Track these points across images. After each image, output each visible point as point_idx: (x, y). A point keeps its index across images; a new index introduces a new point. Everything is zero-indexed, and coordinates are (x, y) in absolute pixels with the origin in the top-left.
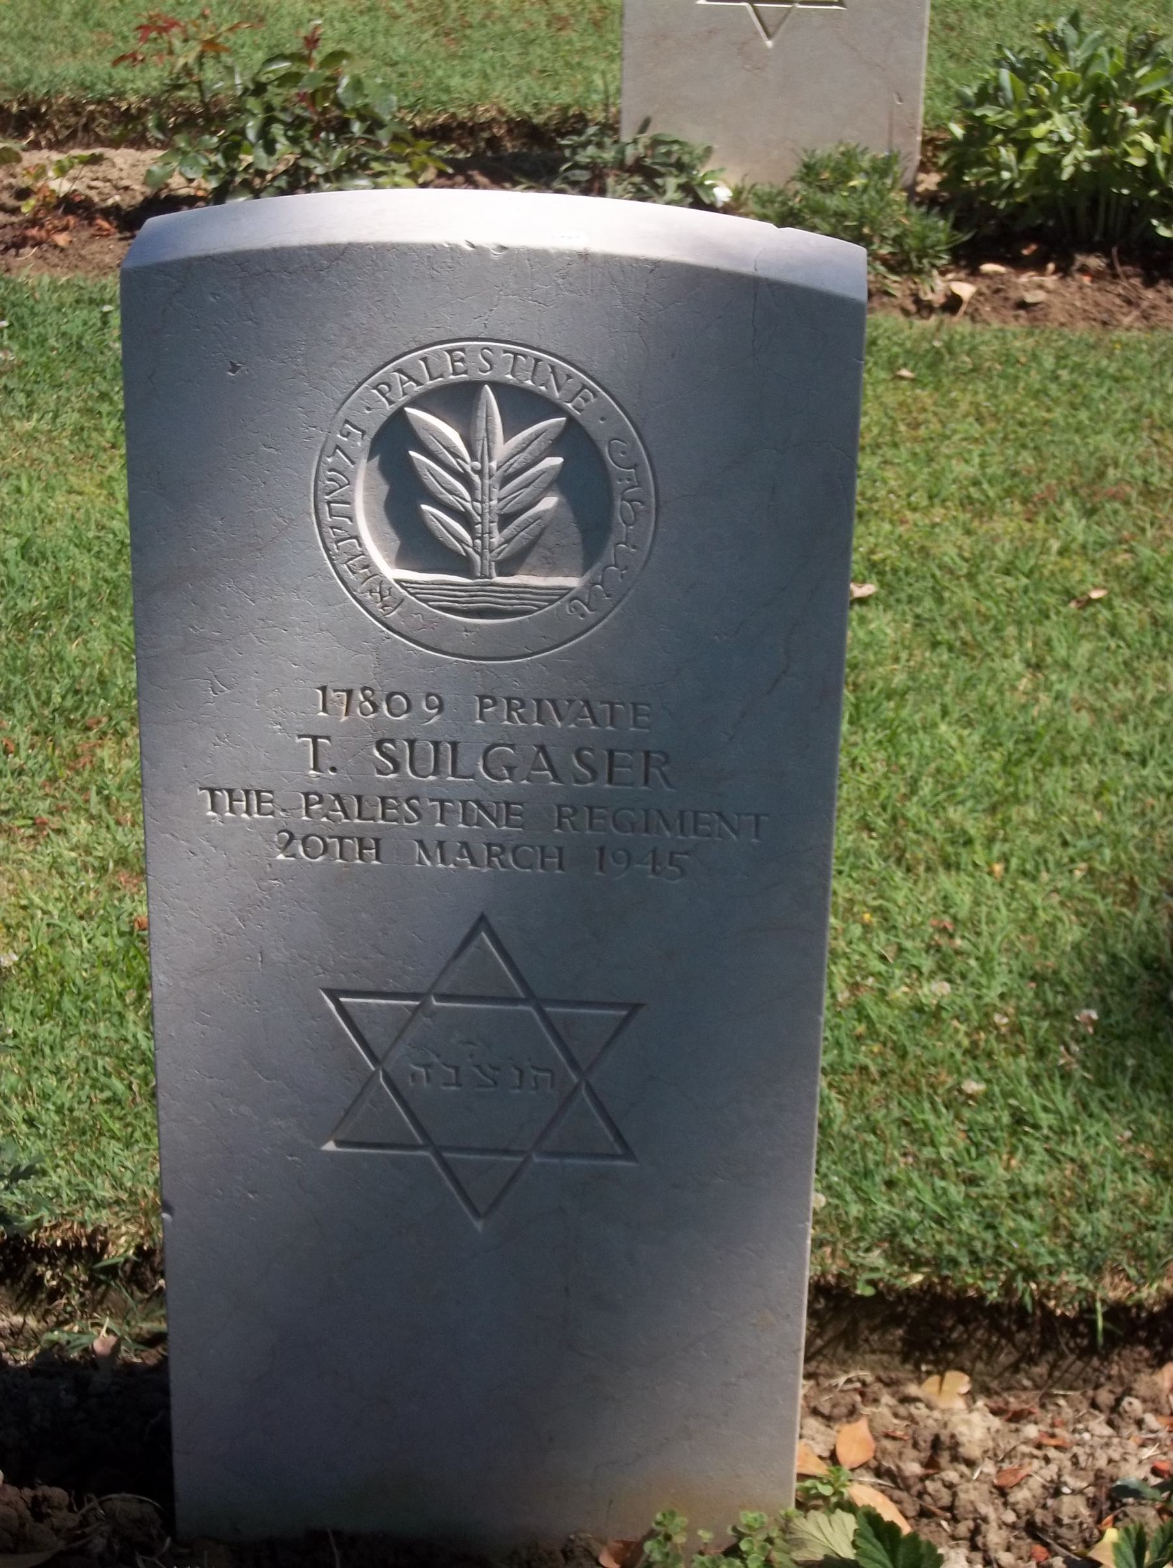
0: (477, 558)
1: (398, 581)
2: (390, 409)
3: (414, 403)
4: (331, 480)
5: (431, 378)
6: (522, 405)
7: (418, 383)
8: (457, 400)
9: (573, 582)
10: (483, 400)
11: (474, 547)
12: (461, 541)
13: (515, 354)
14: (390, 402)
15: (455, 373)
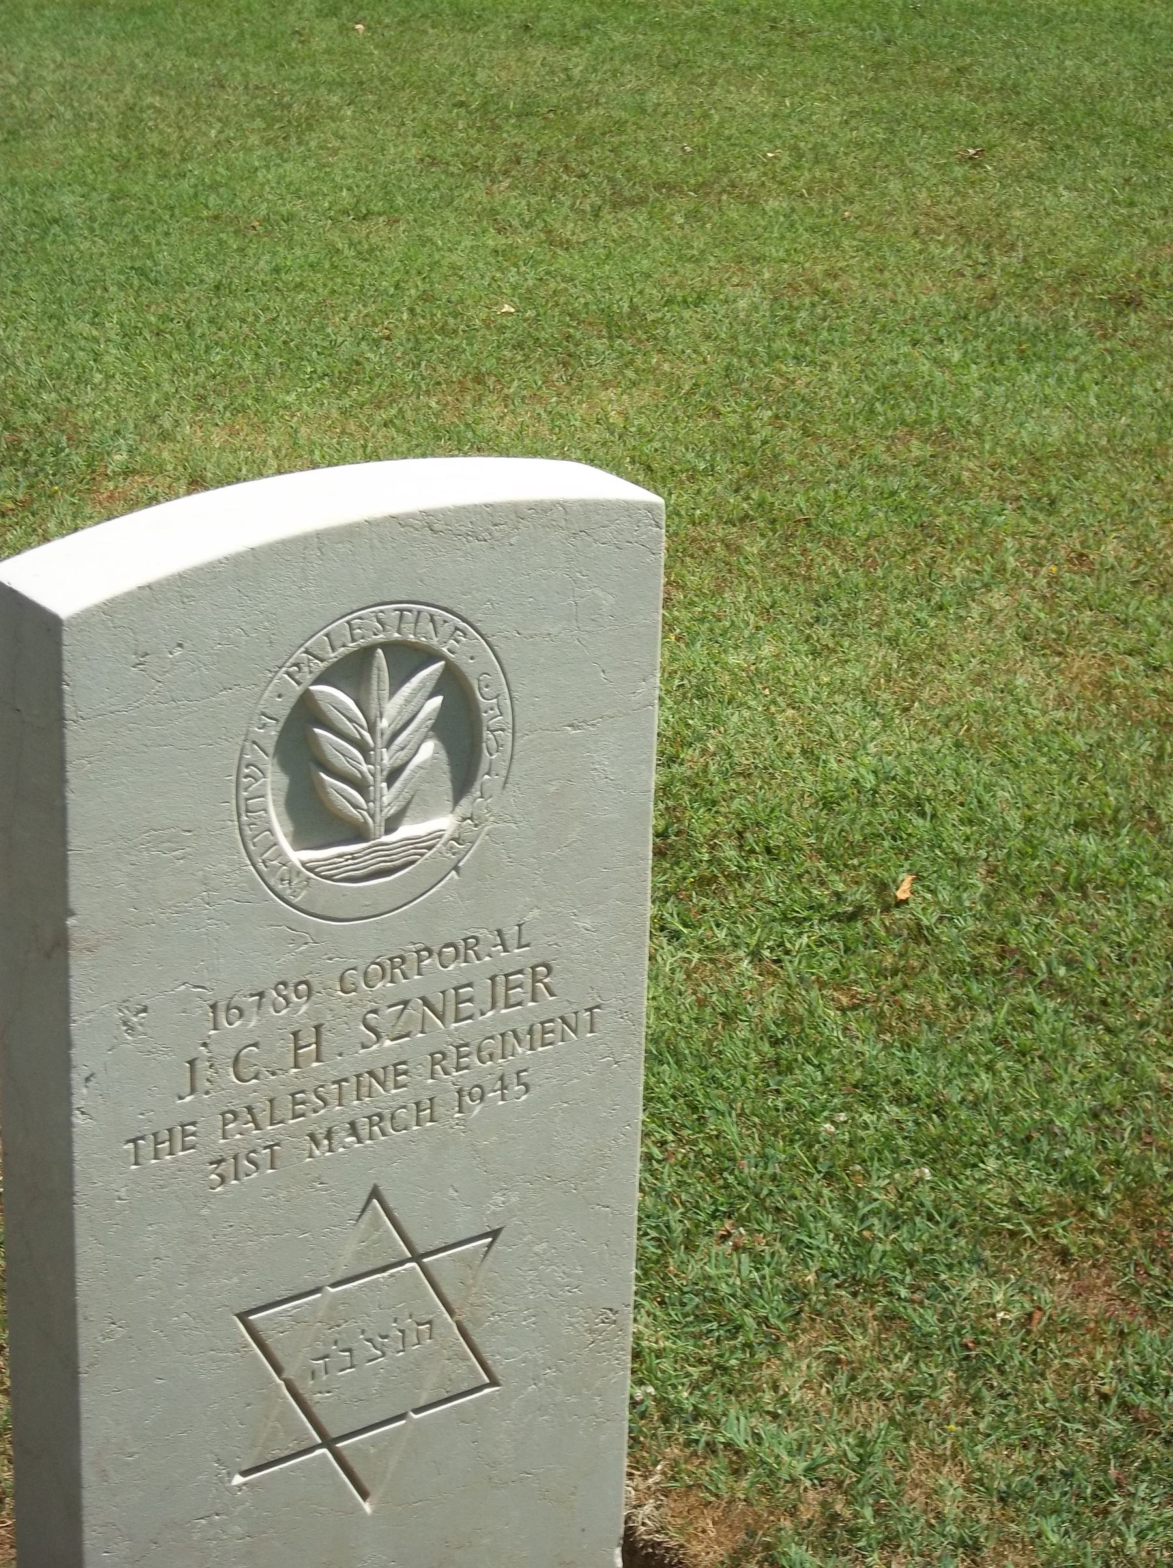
0: (370, 820)
1: (303, 864)
2: (299, 689)
3: (316, 682)
4: (247, 776)
5: (334, 650)
6: (408, 658)
7: (322, 660)
8: (352, 671)
9: (445, 823)
10: (375, 664)
11: (368, 811)
12: (356, 807)
13: (401, 610)
14: (298, 683)
15: (353, 640)
